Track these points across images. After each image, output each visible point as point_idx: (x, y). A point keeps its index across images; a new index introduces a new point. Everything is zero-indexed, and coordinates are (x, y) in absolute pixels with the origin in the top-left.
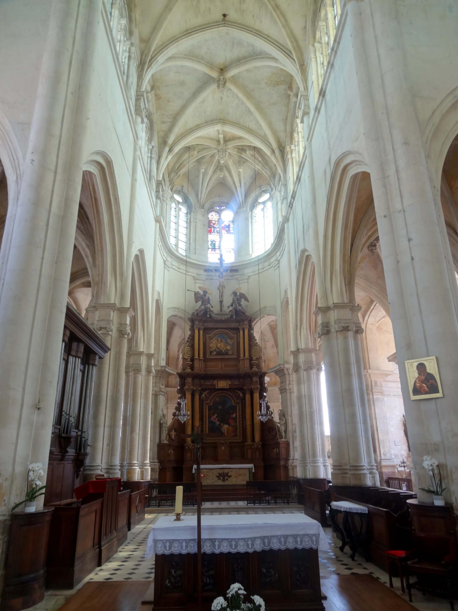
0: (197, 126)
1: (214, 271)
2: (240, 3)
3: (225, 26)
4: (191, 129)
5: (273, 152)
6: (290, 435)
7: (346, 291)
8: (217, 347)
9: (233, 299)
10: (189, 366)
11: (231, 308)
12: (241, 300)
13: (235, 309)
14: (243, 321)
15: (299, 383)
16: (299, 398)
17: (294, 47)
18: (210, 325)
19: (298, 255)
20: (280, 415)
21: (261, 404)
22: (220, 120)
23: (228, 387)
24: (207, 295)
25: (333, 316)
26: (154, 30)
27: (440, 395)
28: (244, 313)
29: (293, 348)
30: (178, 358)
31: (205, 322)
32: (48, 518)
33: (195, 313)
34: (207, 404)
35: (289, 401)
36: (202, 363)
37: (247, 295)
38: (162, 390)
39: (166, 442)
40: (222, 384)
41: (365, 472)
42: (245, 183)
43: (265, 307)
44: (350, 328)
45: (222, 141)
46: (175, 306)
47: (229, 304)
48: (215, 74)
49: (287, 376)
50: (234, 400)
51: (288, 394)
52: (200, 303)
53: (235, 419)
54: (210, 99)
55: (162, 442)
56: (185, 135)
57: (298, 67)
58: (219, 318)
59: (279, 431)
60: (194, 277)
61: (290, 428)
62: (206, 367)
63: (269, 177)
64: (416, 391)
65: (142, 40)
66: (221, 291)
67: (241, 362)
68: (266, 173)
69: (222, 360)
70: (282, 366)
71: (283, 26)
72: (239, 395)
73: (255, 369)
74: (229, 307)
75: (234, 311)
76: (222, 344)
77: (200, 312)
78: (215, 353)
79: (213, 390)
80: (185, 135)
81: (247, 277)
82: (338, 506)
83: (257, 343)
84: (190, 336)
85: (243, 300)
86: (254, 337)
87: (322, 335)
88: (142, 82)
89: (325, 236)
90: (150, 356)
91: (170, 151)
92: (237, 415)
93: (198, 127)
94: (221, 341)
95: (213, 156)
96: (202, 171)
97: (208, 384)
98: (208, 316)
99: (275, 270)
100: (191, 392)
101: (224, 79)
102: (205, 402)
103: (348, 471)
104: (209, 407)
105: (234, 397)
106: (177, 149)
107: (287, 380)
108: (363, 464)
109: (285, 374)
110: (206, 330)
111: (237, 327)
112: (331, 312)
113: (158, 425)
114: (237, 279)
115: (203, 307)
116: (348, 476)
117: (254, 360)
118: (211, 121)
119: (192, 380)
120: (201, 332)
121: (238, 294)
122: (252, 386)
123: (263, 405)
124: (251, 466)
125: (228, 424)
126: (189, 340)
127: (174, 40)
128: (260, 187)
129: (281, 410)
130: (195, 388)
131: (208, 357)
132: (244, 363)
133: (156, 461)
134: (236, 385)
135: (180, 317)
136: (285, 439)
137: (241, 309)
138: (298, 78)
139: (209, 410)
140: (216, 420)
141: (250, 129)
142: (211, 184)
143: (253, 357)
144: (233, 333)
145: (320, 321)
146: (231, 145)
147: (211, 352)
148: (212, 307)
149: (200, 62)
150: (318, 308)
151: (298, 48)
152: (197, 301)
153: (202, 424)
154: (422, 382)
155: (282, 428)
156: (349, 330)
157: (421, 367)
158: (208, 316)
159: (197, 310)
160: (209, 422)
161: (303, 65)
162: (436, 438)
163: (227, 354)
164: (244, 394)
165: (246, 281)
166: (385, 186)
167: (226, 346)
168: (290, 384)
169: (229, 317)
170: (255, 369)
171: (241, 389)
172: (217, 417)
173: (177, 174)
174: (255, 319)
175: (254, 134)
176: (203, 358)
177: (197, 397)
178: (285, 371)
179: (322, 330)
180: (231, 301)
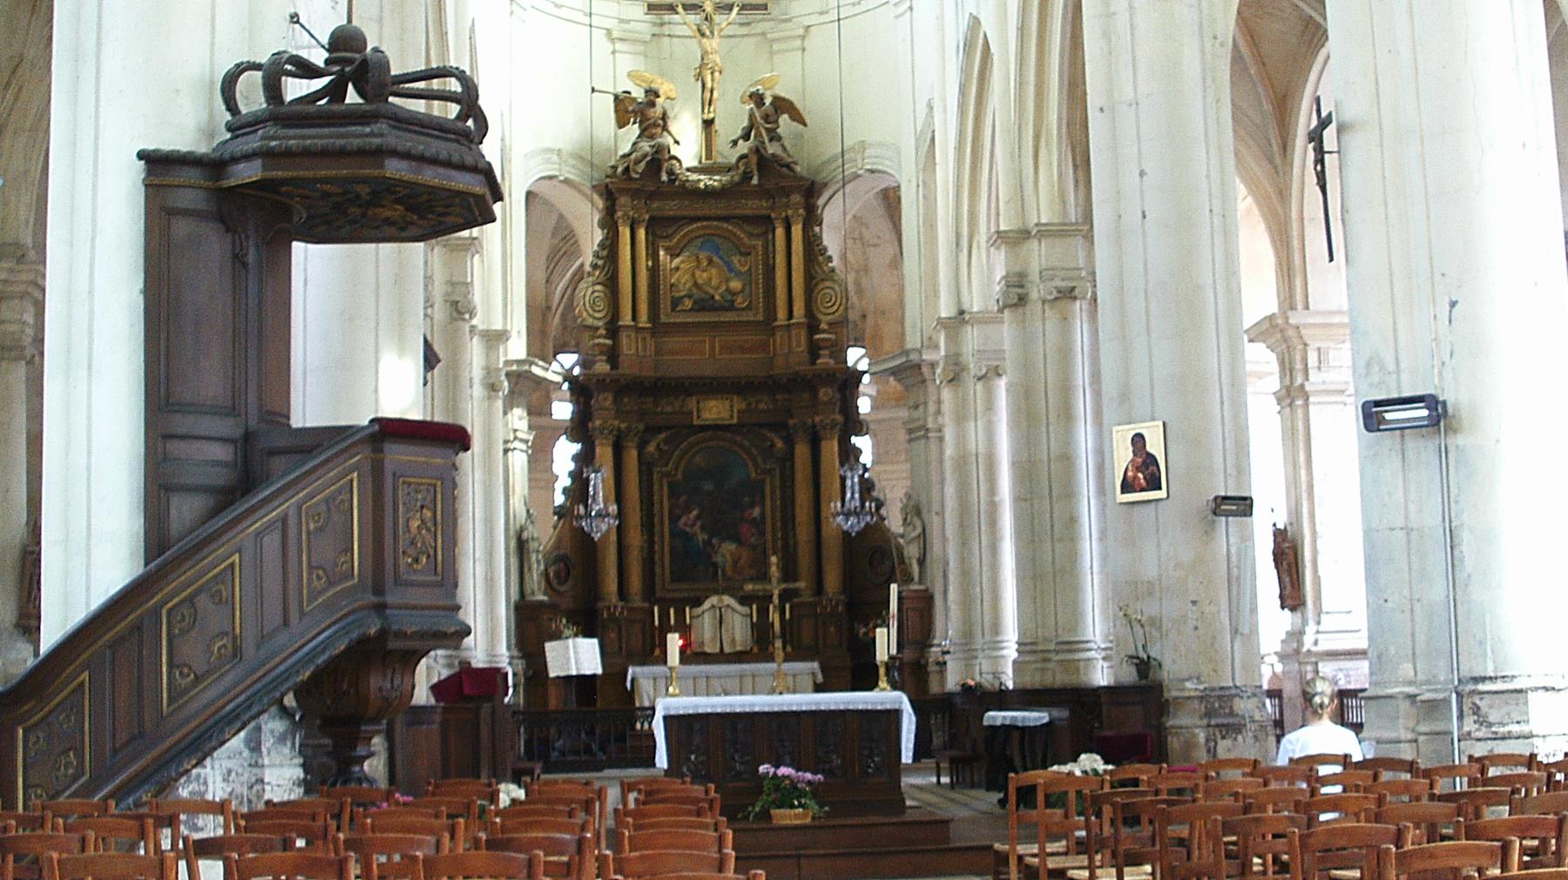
1: (680, 9)
6: (934, 570)
7: (1076, 181)
8: (696, 284)
9: (751, 116)
10: (601, 353)
11: (744, 148)
12: (776, 121)
13: (757, 151)
14: (786, 192)
15: (961, 418)
16: (962, 462)
18: (671, 208)
19: (964, 23)
20: (904, 509)
21: (843, 479)
23: (735, 421)
24: (659, 101)
25: (1037, 255)
27: (1162, 494)
28: (788, 166)
29: (946, 310)
30: (549, 308)
31: (652, 196)
32: (437, 718)
33: (620, 170)
34: (667, 475)
35: (934, 465)
36: (644, 339)
37: (798, 105)
38: (519, 435)
39: (542, 597)
40: (715, 410)
41: (1092, 654)
43: (863, 145)
44: (1077, 292)
46: (549, 144)
47: (739, 133)
49: (931, 388)
50: (756, 465)
51: (933, 445)
52: (633, 130)
53: (759, 524)
55: (529, 598)
58: (705, 181)
59: (902, 560)
60: (609, 31)
61: (936, 549)
62: (657, 353)
64: (1127, 487)
66: (709, 85)
67: (778, 335)
69: (714, 326)
70: (914, 357)
72: (773, 445)
73: (825, 360)
74: (735, 143)
75: (754, 159)
76: (714, 271)
77: (637, 162)
78: (688, 304)
79: (684, 429)
81: (801, 31)
82: (994, 718)
83: (833, 270)
84: (602, 245)
85: (784, 119)
86: (825, 249)
87: (1005, 307)
89: (1022, 30)
90: (495, 339)
92: (766, 509)
94: (710, 261)
97: (669, 409)
98: (664, 178)
99: (897, 17)
100: (611, 439)
102: (656, 469)
103: (1052, 656)
104: (671, 485)
105: (754, 451)
107: (932, 399)
108: (1091, 637)
109: (924, 381)
110: (659, 227)
111: (764, 212)
112: (1033, 244)
113: (513, 543)
114: (763, 34)
115: (646, 146)
116: (1051, 665)
117: (824, 331)
119: (615, 401)
120: (641, 233)
121: (768, 101)
122: (817, 419)
123: (849, 483)
124: (816, 665)
125: (736, 538)
126: (600, 262)
129: (908, 496)
130: (623, 426)
131: (663, 319)
132: (789, 337)
133: (515, 653)
134: (763, 411)
135: (566, 181)
136: (920, 582)
137: (779, 152)
139: (673, 494)
140: (697, 529)
143: (823, 318)
144: (751, 235)
145: (1000, 273)
147: (675, 302)
148: (677, 142)
150: (998, 232)
152: (621, 123)
153: (651, 542)
154: (1138, 469)
155: (912, 551)
156: (1075, 298)
157: (1138, 440)
158: (664, 178)
159: (624, 156)
160: (672, 535)
162: (1150, 571)
163: (730, 307)
164: (790, 442)
165: (798, 43)
166: (1107, 35)
167: (728, 281)
168: (938, 412)
169: (737, 178)
170: (825, 360)
171: (780, 427)
172: (698, 517)
174: (825, 185)
176: (650, 320)
177: (632, 456)
178: (925, 369)
179: (1005, 293)
180: (746, 123)
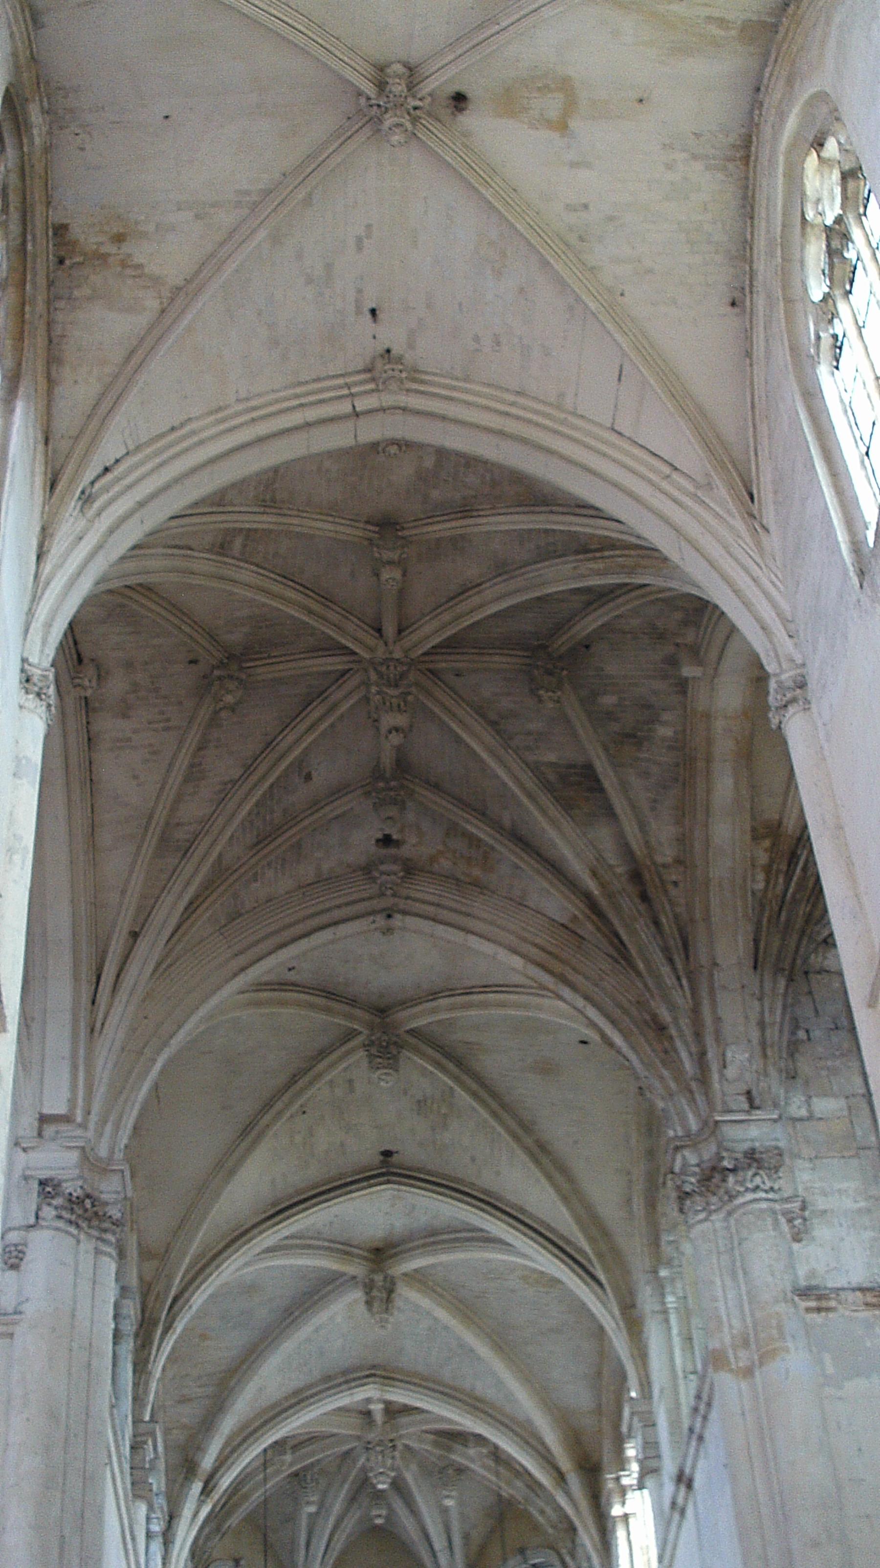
0: (296, 1393)
2: (433, 1130)
3: (388, 1182)
4: (273, 1406)
5: (561, 1477)
17: (600, 1256)
22: (374, 1367)
26: (185, 1224)
42: (466, 1537)
45: (379, 1418)
48: (355, 1269)
54: (340, 1325)
56: (255, 1431)
57: (617, 1312)
63: (554, 1527)
65: (146, 1254)
68: (542, 1512)
71: (565, 1199)
80: (255, 1431)
88: (147, 1383)
91: (206, 1491)
93: (298, 1399)
95: (348, 1453)
96: (312, 1509)
101: (385, 1277)
106: (225, 1482)
118: (344, 1373)
127: (239, 1236)
128: (522, 1551)
138: (620, 1344)
141: (477, 1399)
142: (338, 1545)
146: (409, 1432)
149: (309, 1247)
151: (614, 1258)
161: (633, 1306)
173: (218, 1529)
175: (490, 1416)
